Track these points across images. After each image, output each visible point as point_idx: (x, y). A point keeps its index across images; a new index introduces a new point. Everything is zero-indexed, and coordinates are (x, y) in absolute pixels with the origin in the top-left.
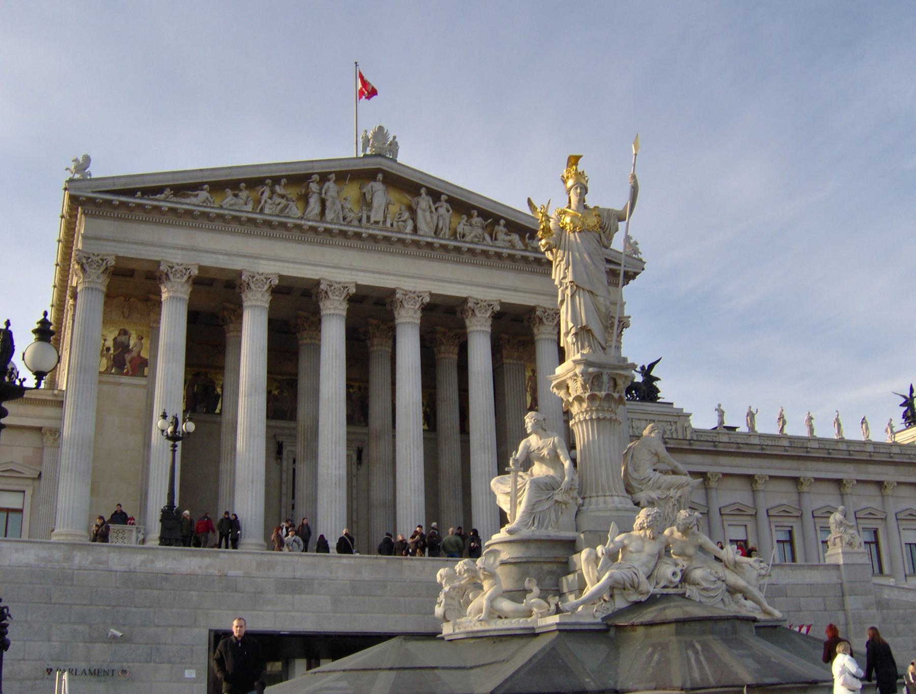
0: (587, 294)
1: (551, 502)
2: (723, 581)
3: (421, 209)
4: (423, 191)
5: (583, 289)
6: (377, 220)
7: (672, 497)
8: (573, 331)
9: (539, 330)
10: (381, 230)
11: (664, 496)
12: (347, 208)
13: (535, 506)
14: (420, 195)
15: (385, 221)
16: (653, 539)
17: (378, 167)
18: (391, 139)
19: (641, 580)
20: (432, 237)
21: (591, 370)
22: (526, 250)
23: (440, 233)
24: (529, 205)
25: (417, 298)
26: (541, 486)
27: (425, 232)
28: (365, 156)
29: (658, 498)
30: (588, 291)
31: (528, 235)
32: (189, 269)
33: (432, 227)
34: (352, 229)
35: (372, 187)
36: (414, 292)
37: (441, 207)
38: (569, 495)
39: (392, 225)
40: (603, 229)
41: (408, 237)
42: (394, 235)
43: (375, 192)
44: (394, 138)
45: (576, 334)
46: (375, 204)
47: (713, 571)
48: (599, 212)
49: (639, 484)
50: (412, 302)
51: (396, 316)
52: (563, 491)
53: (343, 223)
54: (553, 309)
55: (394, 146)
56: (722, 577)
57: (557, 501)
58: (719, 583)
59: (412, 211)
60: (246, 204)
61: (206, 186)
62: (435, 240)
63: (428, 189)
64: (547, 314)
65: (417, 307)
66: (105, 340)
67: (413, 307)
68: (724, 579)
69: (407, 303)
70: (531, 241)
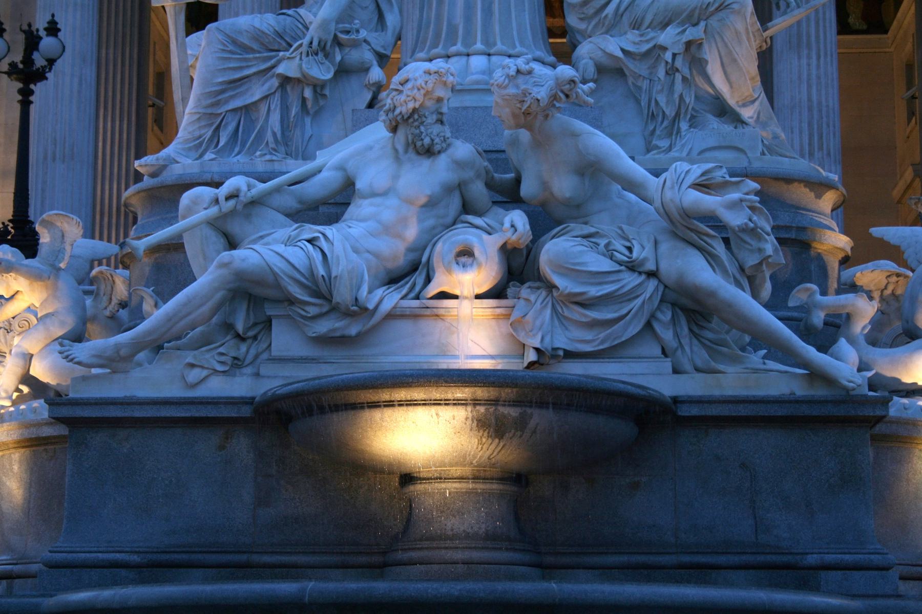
1: (275, 82)
2: (652, 274)
7: (664, 49)
11: (645, 47)
13: (220, 97)
16: (429, 152)
19: (333, 275)
26: (245, 40)
29: (623, 50)
38: (332, 63)
47: (618, 245)
49: (581, 19)
52: (304, 49)
56: (643, 262)
57: (286, 81)
58: (631, 280)
68: (650, 266)
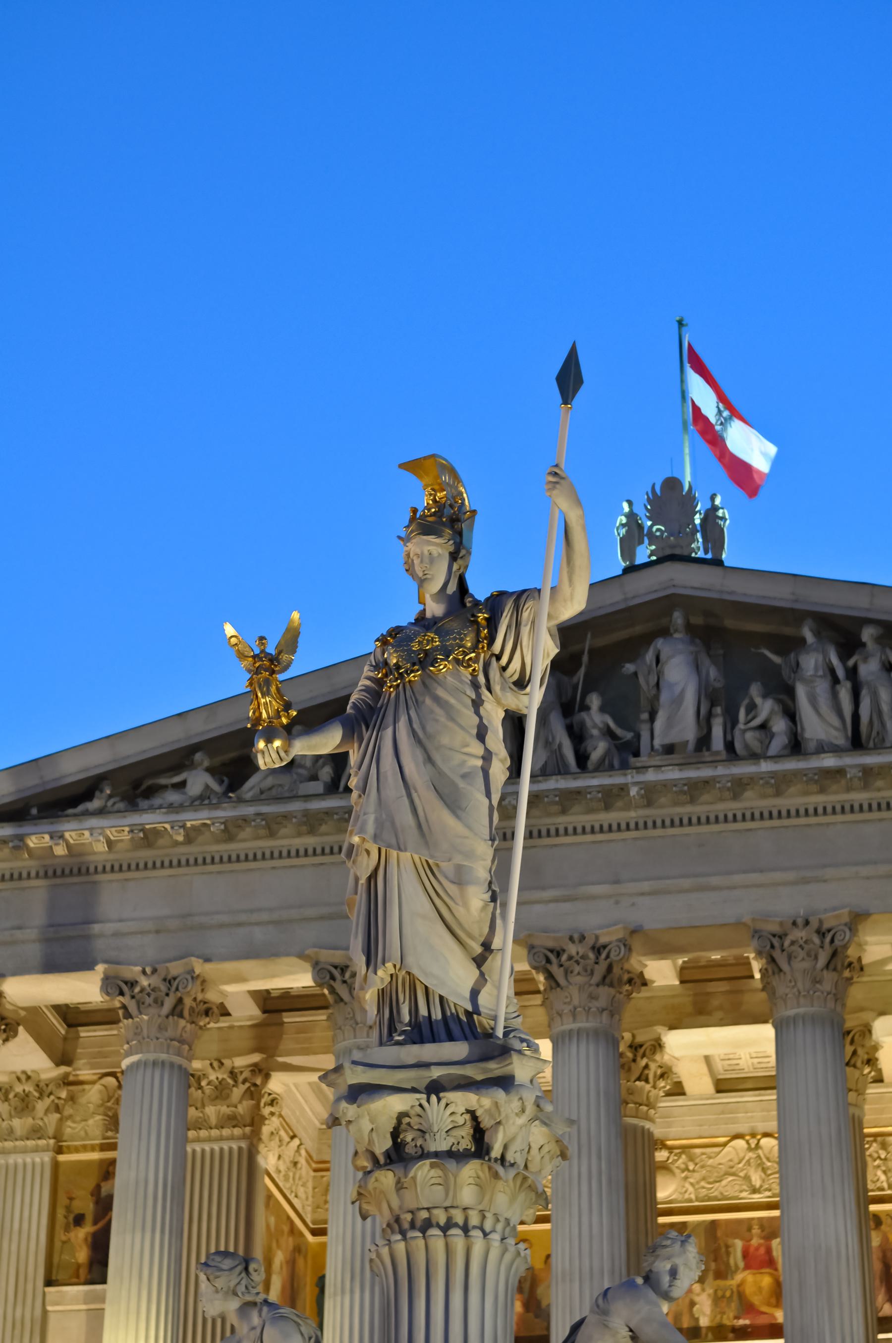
6: (673, 737)
10: (681, 765)
12: (595, 726)
15: (704, 742)
25: (817, 940)
28: (631, 569)
32: (175, 979)
34: (595, 782)
36: (807, 923)
37: (865, 660)
39: (730, 746)
53: (578, 770)
60: (314, 778)
61: (198, 756)
66: (71, 1199)
69: (790, 958)
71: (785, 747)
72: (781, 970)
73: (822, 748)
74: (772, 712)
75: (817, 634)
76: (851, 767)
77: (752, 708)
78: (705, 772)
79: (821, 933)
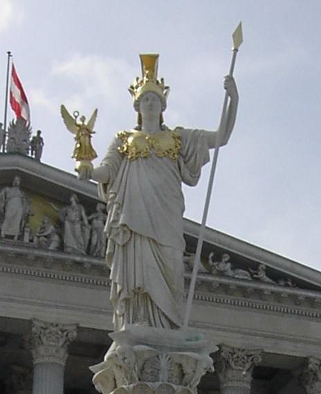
0: (146, 243)
3: (69, 220)
4: (72, 199)
5: (141, 236)
8: (122, 296)
9: (225, 376)
10: (13, 245)
14: (70, 204)
15: (21, 237)
17: (17, 168)
18: (34, 134)
20: (83, 255)
21: (137, 348)
22: (210, 273)
23: (94, 252)
24: (63, 117)
25: (60, 333)
27: (74, 249)
30: (149, 239)
31: (211, 255)
33: (83, 243)
35: (6, 194)
36: (57, 325)
37: (97, 218)
39: (31, 241)
40: (184, 157)
41: (50, 254)
42: (31, 251)
43: (10, 199)
44: (39, 132)
45: (127, 300)
46: (9, 214)
48: (180, 135)
50: (53, 338)
51: (34, 356)
54: (243, 350)
55: (38, 143)
59: (60, 225)
62: (85, 259)
63: (78, 194)
64: (235, 356)
65: (61, 344)
67: (52, 343)
69: (47, 339)
70: (215, 264)
71: (57, 248)
72: (42, 343)
73: (74, 252)
74: (53, 232)
75: (77, 203)
76: (86, 262)
77: (43, 228)
78: (25, 251)
79: (63, 332)
